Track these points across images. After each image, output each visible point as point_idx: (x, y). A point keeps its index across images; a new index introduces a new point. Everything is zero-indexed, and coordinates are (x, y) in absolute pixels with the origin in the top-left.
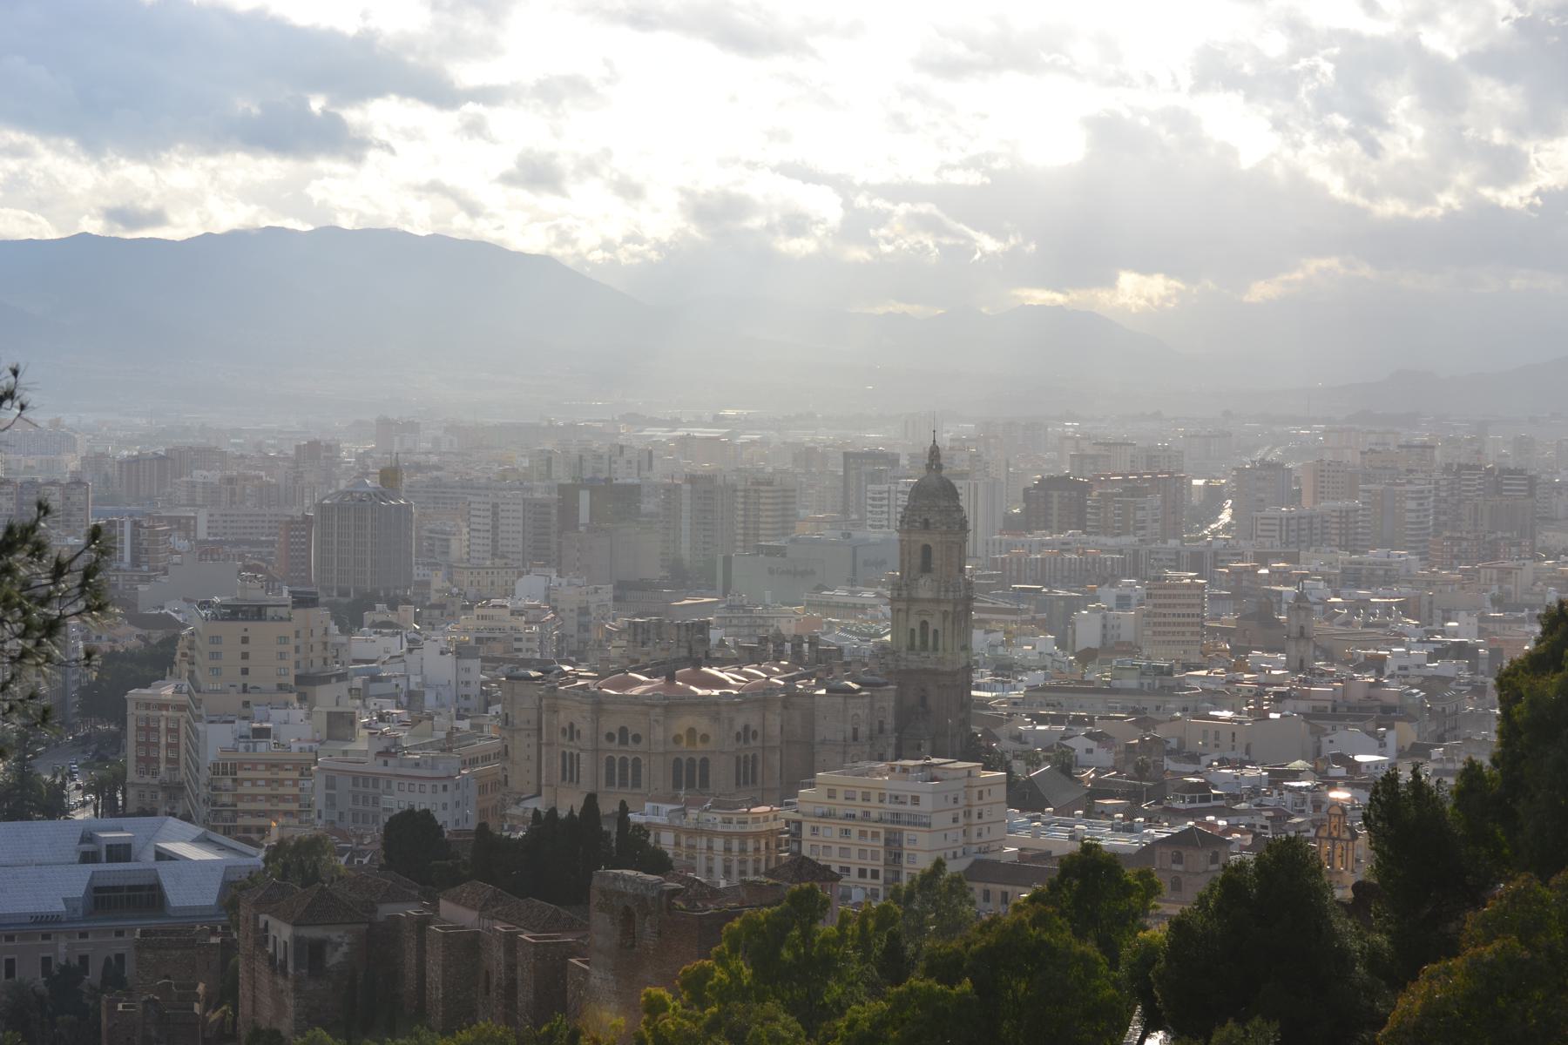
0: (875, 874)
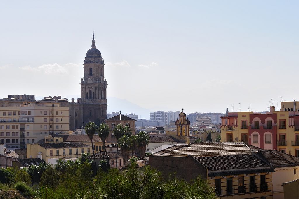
0: (17, 141)
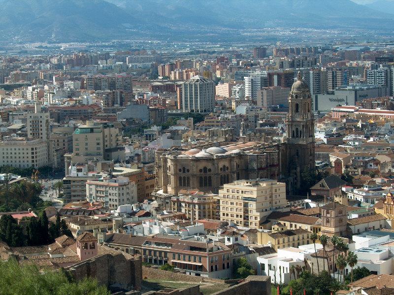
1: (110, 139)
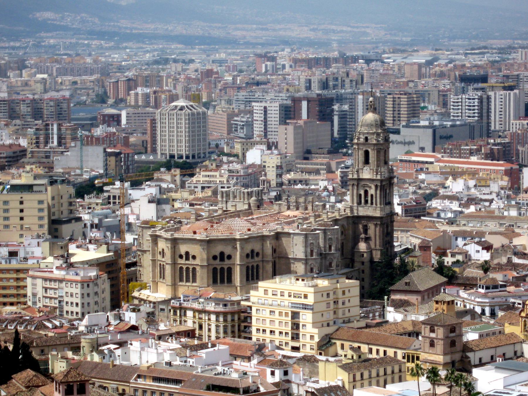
0: (287, 333)
1: (59, 203)
